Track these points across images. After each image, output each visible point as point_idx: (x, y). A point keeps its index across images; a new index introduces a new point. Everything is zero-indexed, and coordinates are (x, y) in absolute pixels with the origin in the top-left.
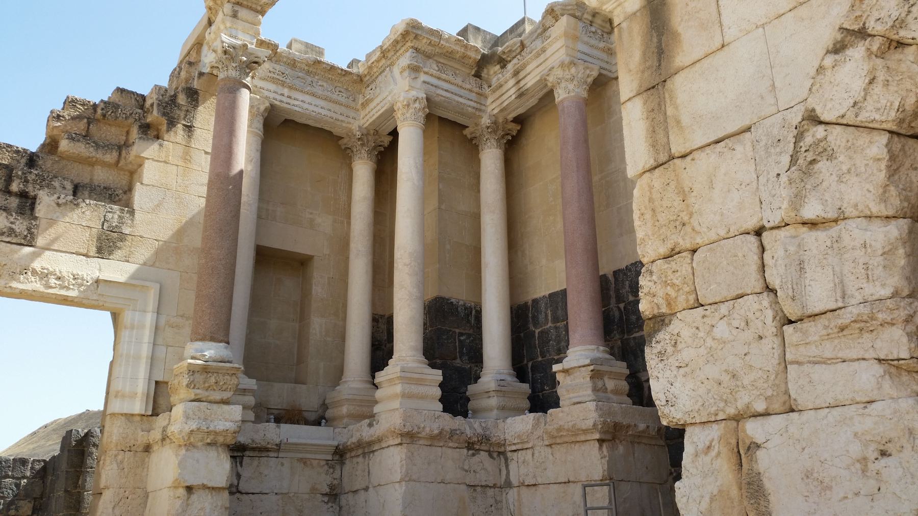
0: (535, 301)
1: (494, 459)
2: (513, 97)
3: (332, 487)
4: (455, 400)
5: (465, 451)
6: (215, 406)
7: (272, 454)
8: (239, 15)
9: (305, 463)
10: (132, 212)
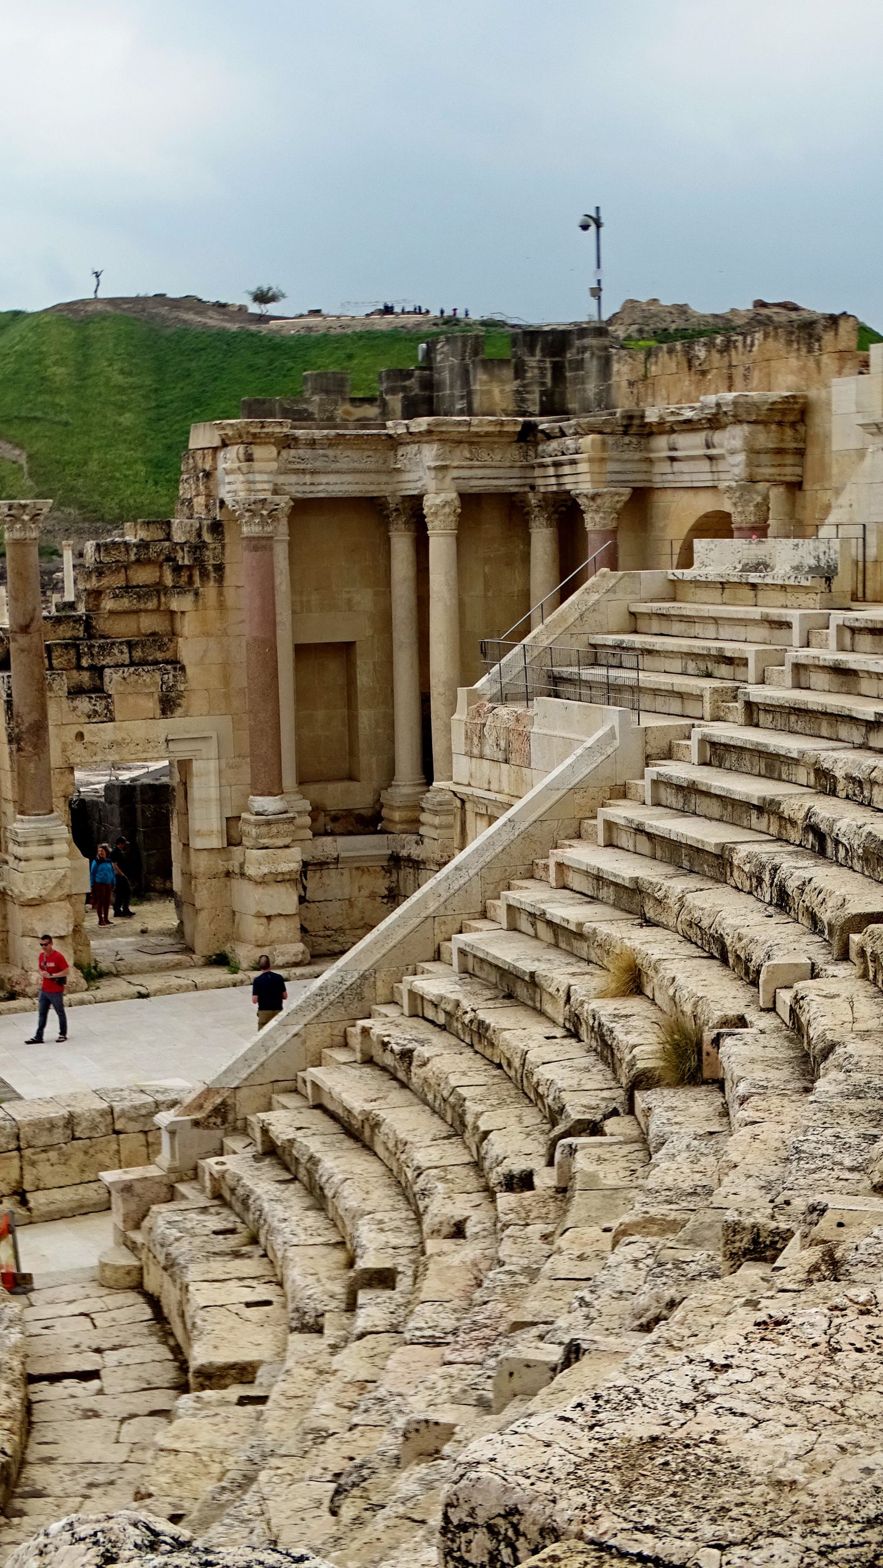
3: (390, 890)
8: (255, 456)
10: (183, 668)
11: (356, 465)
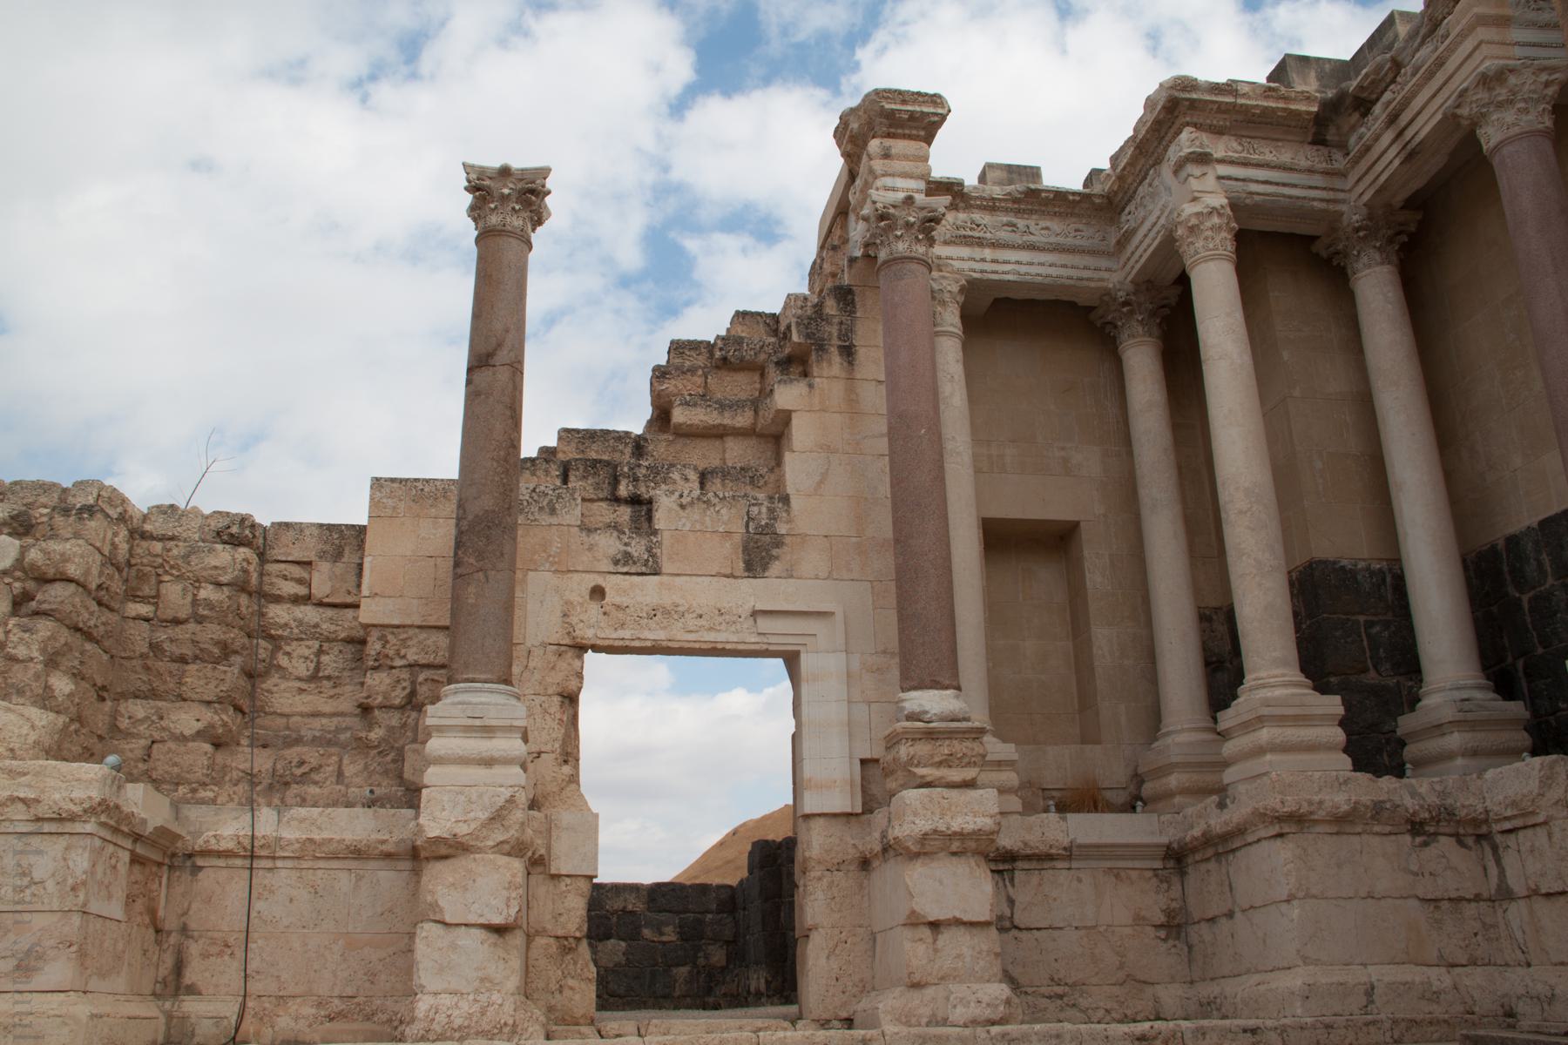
0: (1513, 541)
1: (1470, 848)
2: (1397, 163)
3: (1169, 913)
4: (1375, 745)
5: (1408, 838)
6: (954, 793)
7: (1059, 864)
8: (893, 151)
9: (1117, 876)
11: (1060, 240)
